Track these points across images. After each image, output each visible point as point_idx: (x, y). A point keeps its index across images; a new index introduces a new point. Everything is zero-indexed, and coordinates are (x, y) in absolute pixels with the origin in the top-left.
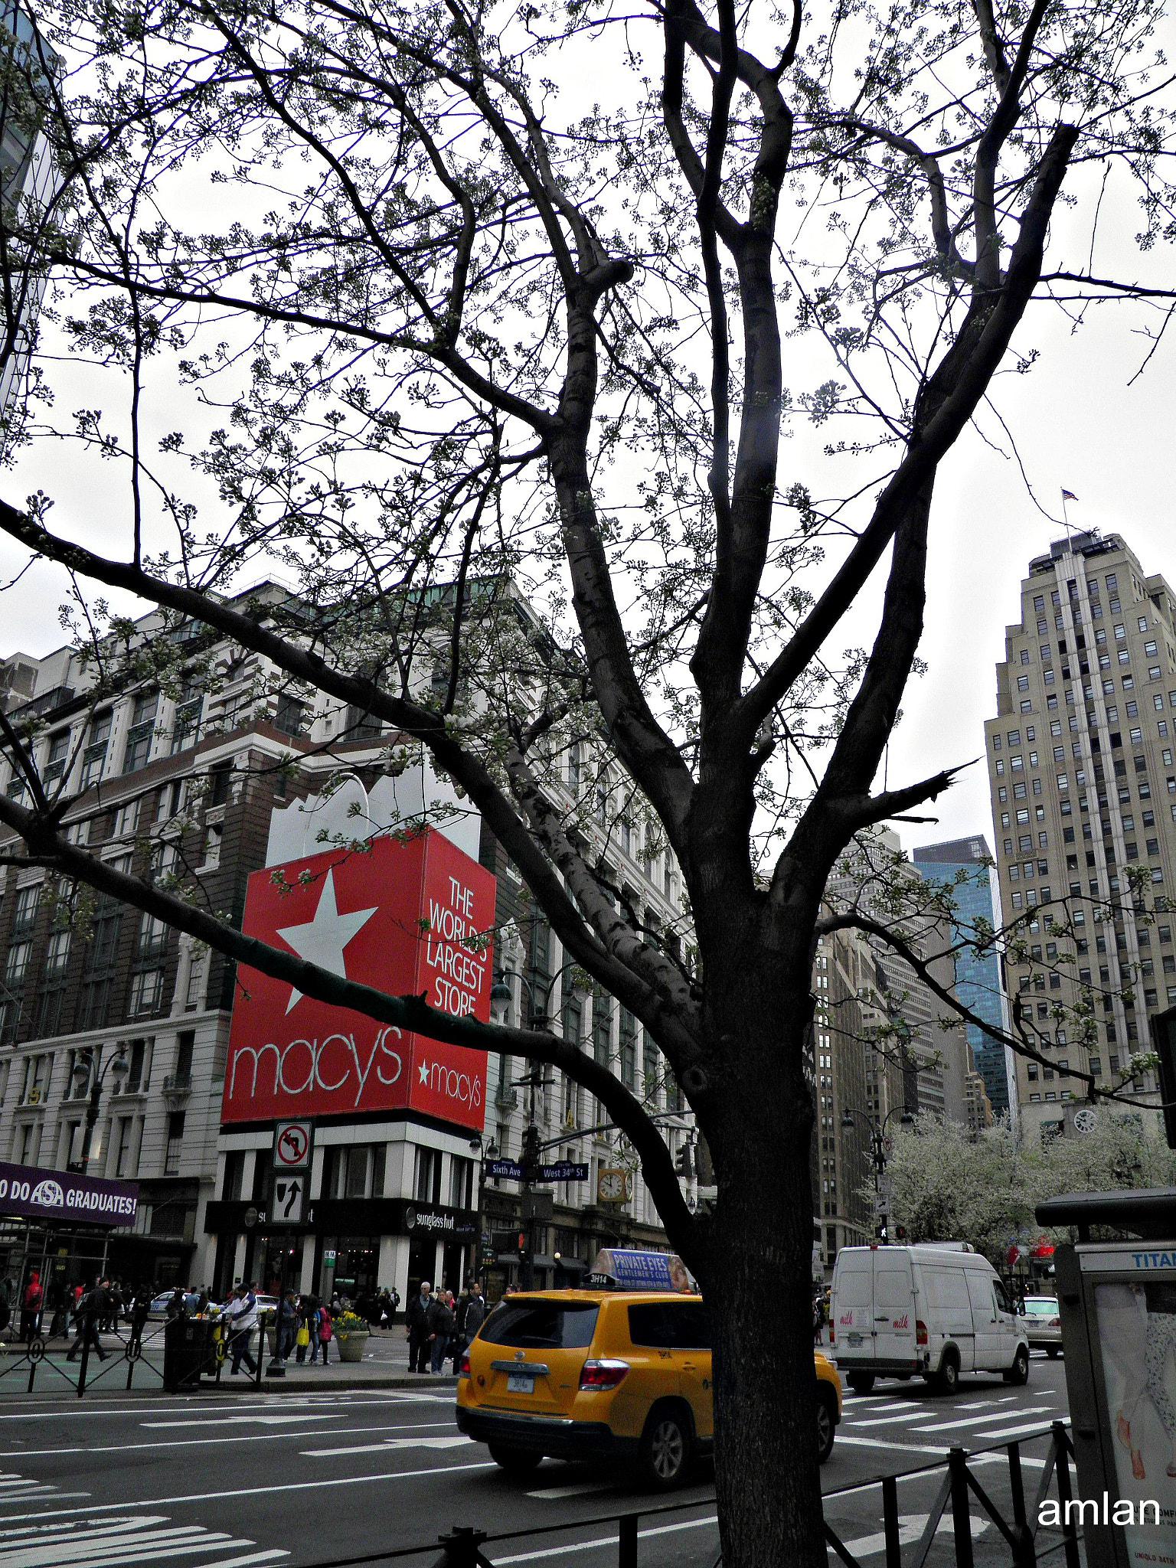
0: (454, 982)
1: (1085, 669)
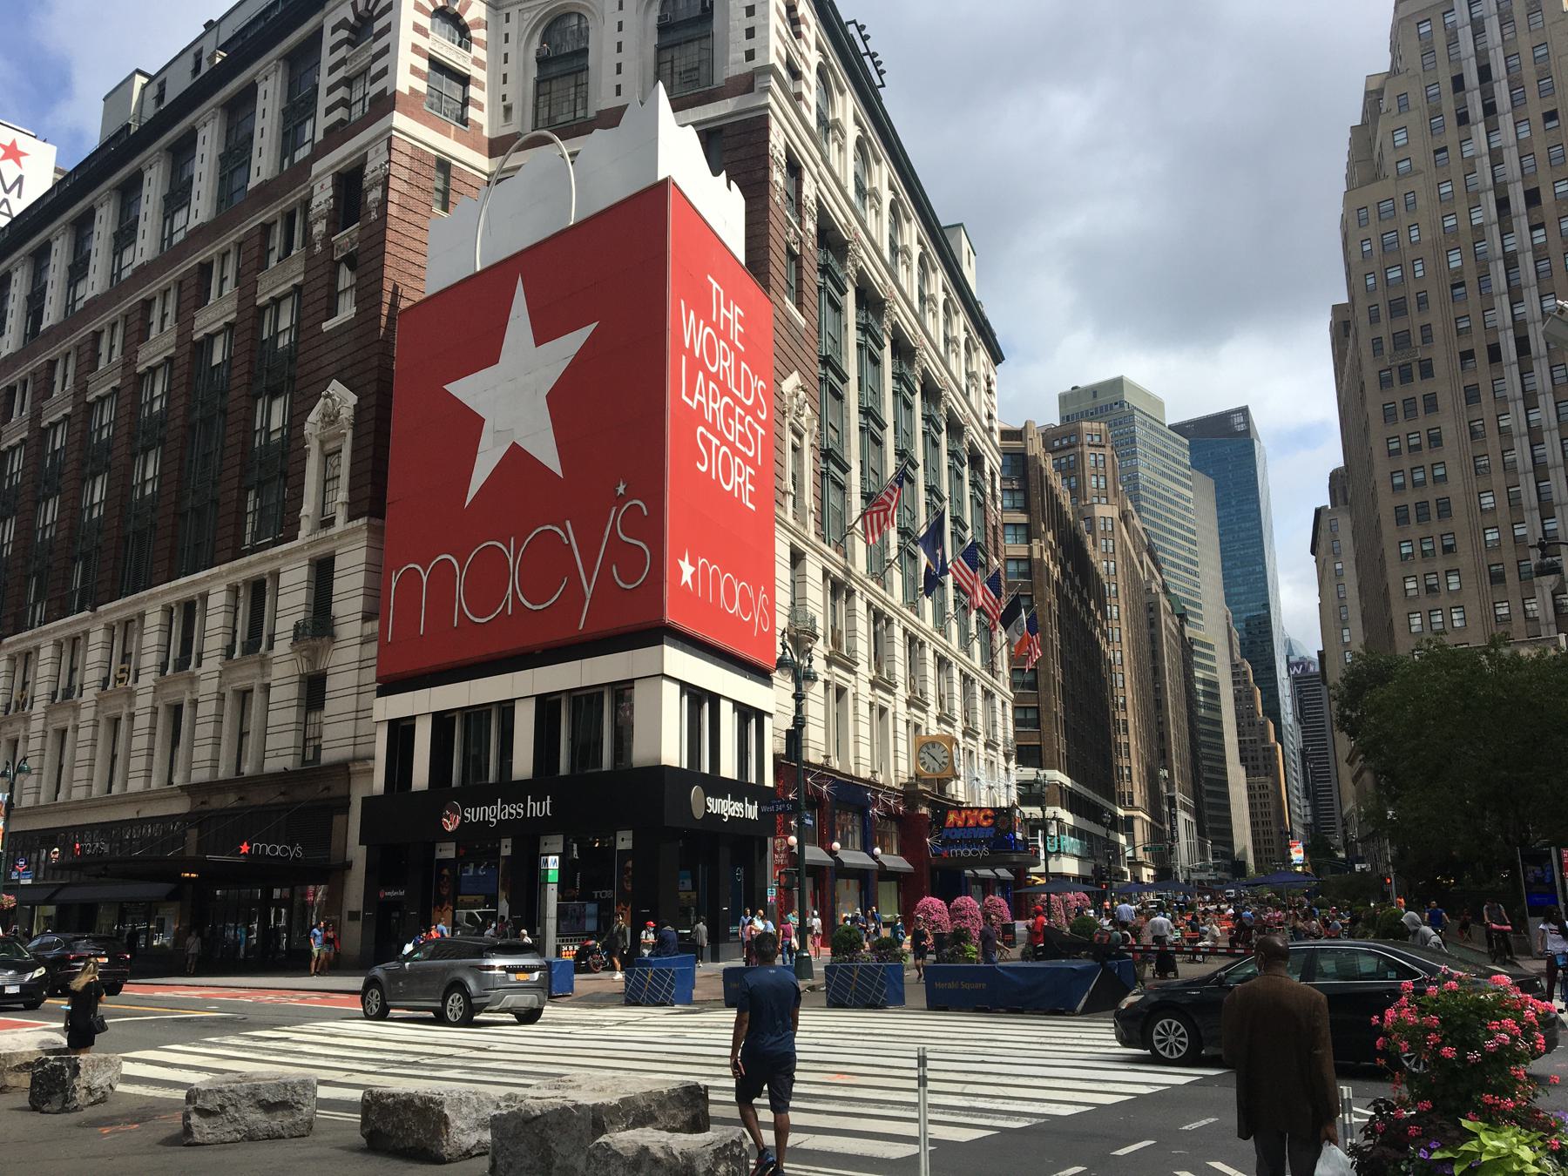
0: (724, 441)
1: (1490, 109)
